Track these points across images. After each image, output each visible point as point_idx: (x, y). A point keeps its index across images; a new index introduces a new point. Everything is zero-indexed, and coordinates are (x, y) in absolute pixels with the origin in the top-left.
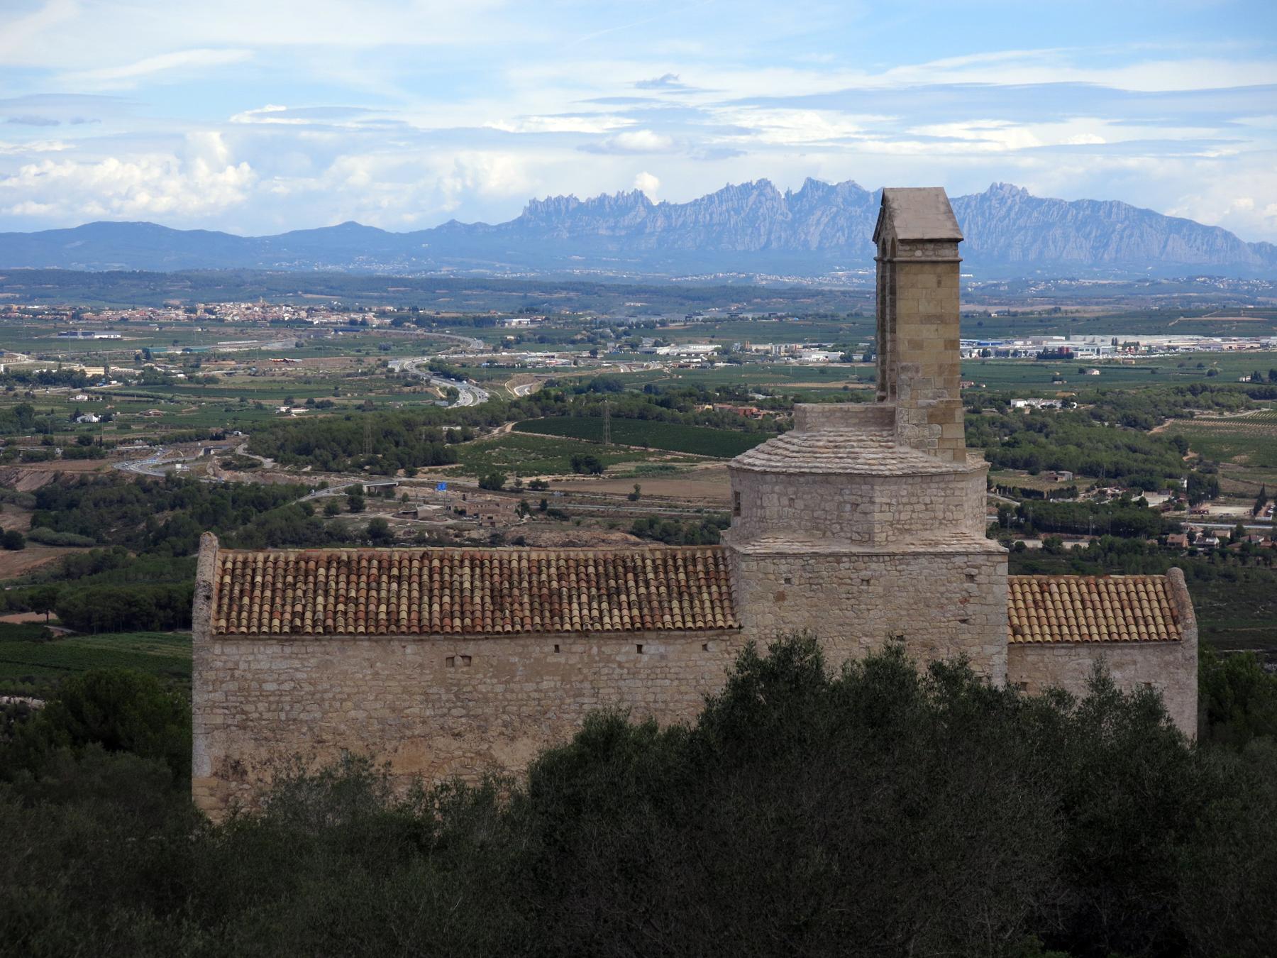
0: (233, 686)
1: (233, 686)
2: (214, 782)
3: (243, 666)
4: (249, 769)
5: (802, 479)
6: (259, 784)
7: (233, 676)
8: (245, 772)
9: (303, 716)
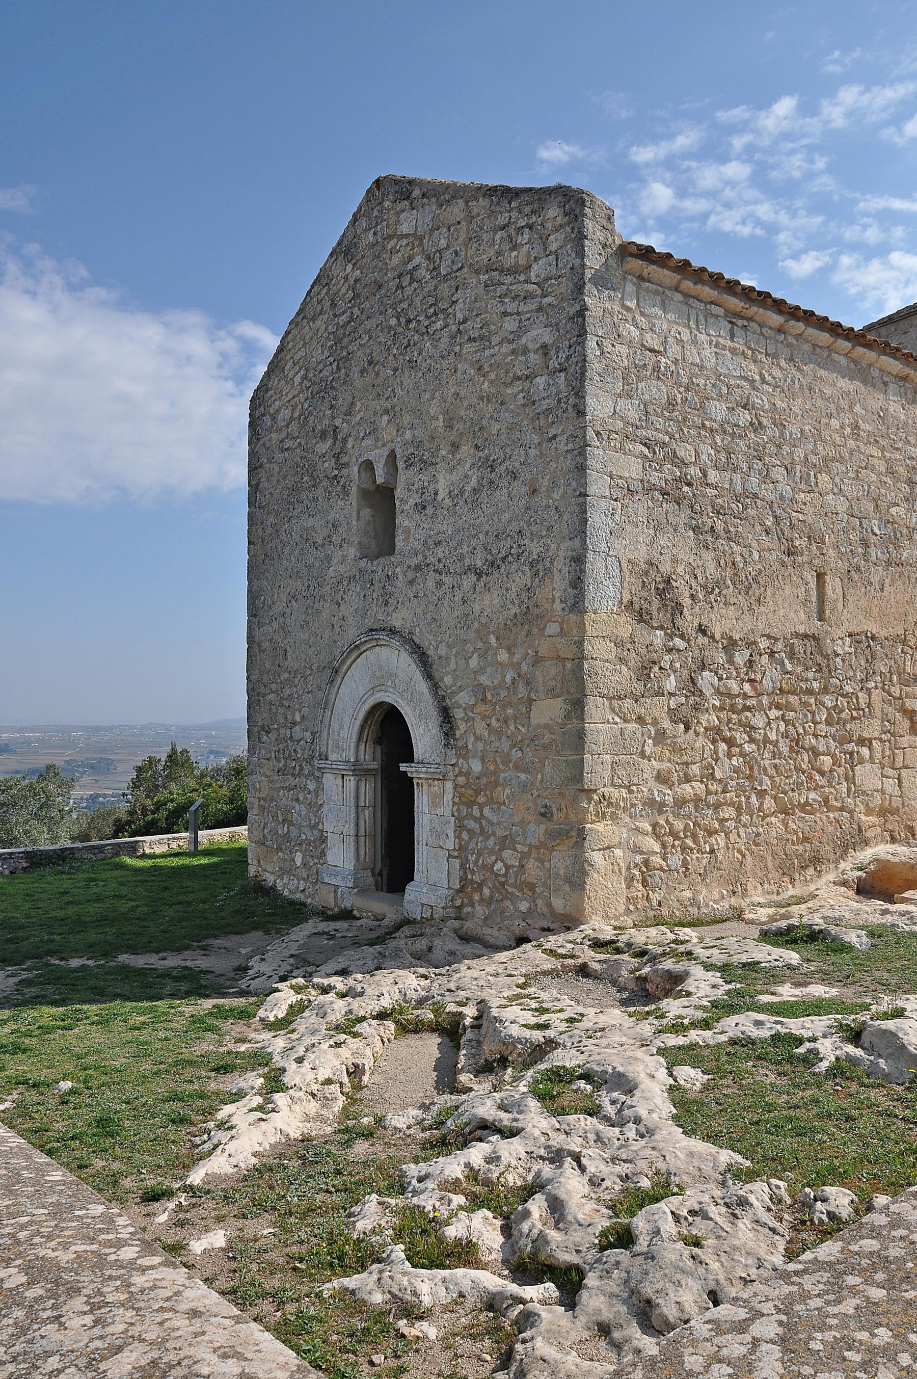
2: (625, 627)
3: (674, 350)
4: (686, 602)
6: (702, 640)
7: (656, 368)
9: (767, 492)
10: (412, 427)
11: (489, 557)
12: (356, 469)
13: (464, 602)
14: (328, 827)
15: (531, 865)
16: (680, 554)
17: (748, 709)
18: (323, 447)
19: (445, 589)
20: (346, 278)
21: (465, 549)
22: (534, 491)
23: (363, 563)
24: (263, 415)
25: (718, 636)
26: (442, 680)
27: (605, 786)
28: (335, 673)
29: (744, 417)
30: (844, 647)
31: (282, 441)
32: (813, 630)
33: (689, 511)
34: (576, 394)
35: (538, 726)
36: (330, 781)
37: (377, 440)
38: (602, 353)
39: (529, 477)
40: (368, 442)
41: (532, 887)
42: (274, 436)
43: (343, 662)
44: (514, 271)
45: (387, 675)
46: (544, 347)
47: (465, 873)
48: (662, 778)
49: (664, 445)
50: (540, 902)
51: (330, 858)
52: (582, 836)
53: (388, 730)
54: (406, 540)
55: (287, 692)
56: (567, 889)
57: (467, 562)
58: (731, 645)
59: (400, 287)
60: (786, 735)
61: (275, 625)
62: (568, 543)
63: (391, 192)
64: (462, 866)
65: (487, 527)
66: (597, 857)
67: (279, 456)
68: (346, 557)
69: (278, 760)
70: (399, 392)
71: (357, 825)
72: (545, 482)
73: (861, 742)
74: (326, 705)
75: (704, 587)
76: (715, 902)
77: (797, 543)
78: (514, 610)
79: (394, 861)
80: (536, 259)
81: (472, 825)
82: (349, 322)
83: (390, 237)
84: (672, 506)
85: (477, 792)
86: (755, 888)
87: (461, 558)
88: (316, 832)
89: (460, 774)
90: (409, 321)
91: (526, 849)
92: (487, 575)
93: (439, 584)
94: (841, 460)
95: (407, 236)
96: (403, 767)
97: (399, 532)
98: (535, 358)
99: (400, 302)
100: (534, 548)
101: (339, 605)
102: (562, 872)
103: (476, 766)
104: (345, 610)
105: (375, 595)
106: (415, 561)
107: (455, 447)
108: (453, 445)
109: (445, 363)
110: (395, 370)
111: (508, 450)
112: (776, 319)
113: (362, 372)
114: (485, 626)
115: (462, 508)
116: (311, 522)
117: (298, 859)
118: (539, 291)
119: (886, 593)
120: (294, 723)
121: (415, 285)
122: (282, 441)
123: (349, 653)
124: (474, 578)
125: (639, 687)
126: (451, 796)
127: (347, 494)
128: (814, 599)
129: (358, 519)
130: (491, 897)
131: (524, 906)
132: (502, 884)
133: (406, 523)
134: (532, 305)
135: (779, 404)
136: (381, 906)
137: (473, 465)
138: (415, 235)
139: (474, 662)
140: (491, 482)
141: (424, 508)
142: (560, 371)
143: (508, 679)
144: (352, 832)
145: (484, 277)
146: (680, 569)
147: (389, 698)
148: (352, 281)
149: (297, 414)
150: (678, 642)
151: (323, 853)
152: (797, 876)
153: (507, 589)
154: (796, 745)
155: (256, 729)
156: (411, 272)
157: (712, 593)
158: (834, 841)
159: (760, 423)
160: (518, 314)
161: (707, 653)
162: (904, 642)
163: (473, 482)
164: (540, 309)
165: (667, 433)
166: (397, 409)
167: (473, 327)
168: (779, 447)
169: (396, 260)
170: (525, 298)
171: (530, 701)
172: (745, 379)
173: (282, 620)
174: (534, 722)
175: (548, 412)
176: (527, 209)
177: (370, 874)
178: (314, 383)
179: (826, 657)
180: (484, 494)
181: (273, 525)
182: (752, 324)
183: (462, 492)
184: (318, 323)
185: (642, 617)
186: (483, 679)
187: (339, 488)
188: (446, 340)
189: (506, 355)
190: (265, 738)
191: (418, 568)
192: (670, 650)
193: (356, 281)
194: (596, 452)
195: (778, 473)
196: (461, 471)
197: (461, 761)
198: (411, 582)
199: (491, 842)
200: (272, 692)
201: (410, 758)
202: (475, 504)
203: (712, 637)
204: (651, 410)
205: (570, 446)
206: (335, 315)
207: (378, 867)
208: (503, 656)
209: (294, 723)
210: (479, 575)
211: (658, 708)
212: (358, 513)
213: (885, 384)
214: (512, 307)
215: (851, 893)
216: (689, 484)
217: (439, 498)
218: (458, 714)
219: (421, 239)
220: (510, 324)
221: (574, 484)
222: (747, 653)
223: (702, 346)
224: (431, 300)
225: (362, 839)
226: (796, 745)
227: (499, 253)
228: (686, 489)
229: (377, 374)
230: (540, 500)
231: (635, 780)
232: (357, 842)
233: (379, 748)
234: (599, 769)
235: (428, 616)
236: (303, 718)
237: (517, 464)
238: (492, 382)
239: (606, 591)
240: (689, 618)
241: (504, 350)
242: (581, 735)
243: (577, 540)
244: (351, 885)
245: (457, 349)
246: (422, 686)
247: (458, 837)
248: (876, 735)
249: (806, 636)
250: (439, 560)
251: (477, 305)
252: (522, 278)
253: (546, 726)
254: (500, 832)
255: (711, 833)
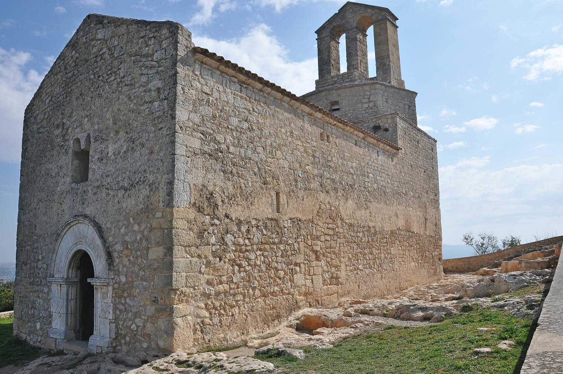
0: (208, 111)
1: (208, 111)
2: (192, 214)
3: (216, 94)
4: (220, 203)
5: (390, 90)
6: (227, 220)
7: (208, 101)
8: (216, 206)
9: (255, 157)
10: (98, 124)
11: (131, 182)
12: (72, 142)
13: (119, 203)
14: (53, 310)
15: (149, 325)
16: (217, 182)
17: (247, 251)
18: (58, 132)
19: (110, 197)
20: (72, 57)
21: (120, 178)
22: (152, 152)
23: (73, 185)
24: (31, 117)
25: (234, 219)
26: (108, 239)
27: (183, 287)
28: (58, 236)
29: (246, 125)
30: (288, 224)
31: (39, 129)
32: (275, 217)
33: (221, 164)
34: (172, 110)
35: (152, 260)
36: (55, 288)
37: (82, 129)
38: (184, 93)
39: (150, 146)
40: (78, 130)
41: (149, 336)
42: (35, 126)
43: (62, 231)
44: (146, 56)
45: (81, 237)
46: (158, 89)
47: (118, 330)
48: (209, 283)
49: (210, 134)
50: (152, 343)
51: (54, 325)
52: (172, 310)
53: (82, 262)
54: (93, 174)
55: (36, 245)
56: (166, 336)
57: (121, 184)
58: (239, 223)
59: (96, 62)
60: (264, 262)
61: (31, 214)
62: (166, 176)
63: (94, 21)
64: (116, 327)
65: (130, 169)
66: (179, 321)
67: (37, 136)
68: (65, 182)
69: (30, 278)
70: (93, 107)
71: (67, 308)
72: (157, 149)
73: (296, 264)
74: (54, 251)
75: (228, 197)
76: (235, 338)
77: (268, 179)
78: (142, 206)
79: (84, 325)
80: (156, 51)
81: (121, 307)
82: (72, 76)
83: (93, 40)
84: (214, 161)
85: (123, 291)
86: (252, 331)
87: (118, 183)
88: (47, 312)
89: (116, 283)
90: (99, 77)
91: (146, 318)
92: (129, 190)
93: (108, 194)
94: (286, 145)
95: (100, 40)
96: (89, 280)
97: (90, 170)
98: (154, 94)
99: (96, 68)
100: (151, 178)
101: (61, 204)
102: (163, 328)
103: (123, 279)
104: (65, 207)
105: (78, 200)
106: (97, 184)
107: (117, 132)
108: (116, 131)
109: (114, 95)
110: (92, 98)
111: (141, 134)
112: (259, 86)
113: (77, 99)
114: (128, 214)
115: (119, 160)
116: (50, 166)
117: (38, 326)
118: (157, 65)
119: (305, 201)
120: (39, 260)
121: (103, 61)
122: (39, 129)
123: (65, 227)
124: (123, 192)
125: (198, 242)
126: (111, 294)
127: (67, 153)
128: (275, 203)
129: (72, 164)
130: (130, 341)
131: (145, 345)
132: (135, 335)
133: (94, 167)
134: (154, 71)
135: (260, 120)
136: (78, 348)
137: (124, 141)
138: (104, 39)
139: (123, 230)
140: (133, 148)
141: (102, 160)
142: (165, 99)
143: (138, 238)
144: (65, 312)
145: (133, 58)
146: (217, 189)
147: (83, 247)
148: (75, 59)
149: (46, 117)
150: (216, 221)
151: (50, 323)
152: (270, 324)
153: (139, 197)
154: (269, 266)
155: (20, 263)
156: (101, 55)
157: (231, 200)
158: (286, 308)
159: (252, 128)
160: (148, 74)
161: (229, 226)
162: (312, 222)
163: (125, 148)
164: (157, 73)
165: (212, 129)
166: (92, 115)
167: (128, 80)
168: (260, 138)
169: (95, 50)
170: (151, 68)
171: (148, 249)
172: (246, 109)
173: (35, 211)
174: (150, 258)
175: (159, 117)
176: (154, 30)
177: (73, 332)
178: (55, 103)
179: (281, 228)
180: (129, 154)
181: (33, 167)
182: (250, 87)
183: (119, 153)
184: (58, 76)
185: (200, 210)
186: (127, 238)
187: (64, 151)
188: (115, 85)
189: (141, 92)
190: (24, 267)
191: (98, 187)
192: (212, 225)
193: (77, 58)
194: (180, 135)
195: (260, 149)
196: (119, 143)
197: (116, 277)
198: (95, 194)
199: (130, 315)
200: (29, 245)
201: (92, 275)
202: (125, 158)
203: (231, 219)
204: (205, 119)
205: (168, 132)
206: (66, 73)
207: (78, 328)
208: (136, 227)
209: (39, 260)
210: (126, 190)
211: (207, 251)
212: (72, 162)
213: (303, 116)
214: (145, 71)
215: (294, 330)
216: (222, 152)
217: (109, 155)
218: (115, 255)
219: (106, 41)
220: (144, 79)
221: (169, 149)
222: (247, 226)
223: (228, 95)
224: (109, 68)
225: (69, 315)
226: (269, 266)
227: (140, 48)
228: (220, 154)
229: (84, 100)
230: (154, 156)
231: (197, 284)
232: (67, 317)
233: (79, 271)
234: (179, 279)
235: (102, 209)
236: (43, 257)
237: (145, 141)
238: (135, 104)
239: (183, 198)
240: (221, 211)
241: (140, 90)
242: (171, 263)
243: (170, 175)
244: (63, 338)
245: (120, 89)
246: (98, 242)
247: (114, 313)
248: (302, 261)
249: (272, 219)
250: (108, 184)
251: (130, 70)
252: (150, 59)
253: (155, 260)
254: (134, 310)
255: (232, 307)
